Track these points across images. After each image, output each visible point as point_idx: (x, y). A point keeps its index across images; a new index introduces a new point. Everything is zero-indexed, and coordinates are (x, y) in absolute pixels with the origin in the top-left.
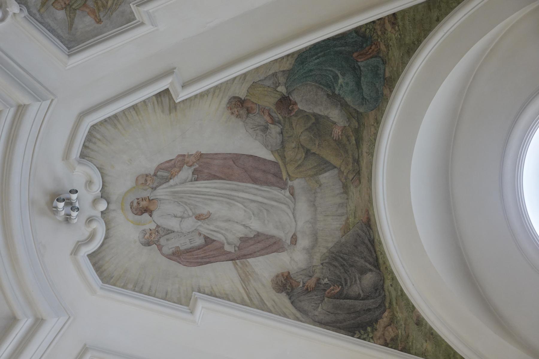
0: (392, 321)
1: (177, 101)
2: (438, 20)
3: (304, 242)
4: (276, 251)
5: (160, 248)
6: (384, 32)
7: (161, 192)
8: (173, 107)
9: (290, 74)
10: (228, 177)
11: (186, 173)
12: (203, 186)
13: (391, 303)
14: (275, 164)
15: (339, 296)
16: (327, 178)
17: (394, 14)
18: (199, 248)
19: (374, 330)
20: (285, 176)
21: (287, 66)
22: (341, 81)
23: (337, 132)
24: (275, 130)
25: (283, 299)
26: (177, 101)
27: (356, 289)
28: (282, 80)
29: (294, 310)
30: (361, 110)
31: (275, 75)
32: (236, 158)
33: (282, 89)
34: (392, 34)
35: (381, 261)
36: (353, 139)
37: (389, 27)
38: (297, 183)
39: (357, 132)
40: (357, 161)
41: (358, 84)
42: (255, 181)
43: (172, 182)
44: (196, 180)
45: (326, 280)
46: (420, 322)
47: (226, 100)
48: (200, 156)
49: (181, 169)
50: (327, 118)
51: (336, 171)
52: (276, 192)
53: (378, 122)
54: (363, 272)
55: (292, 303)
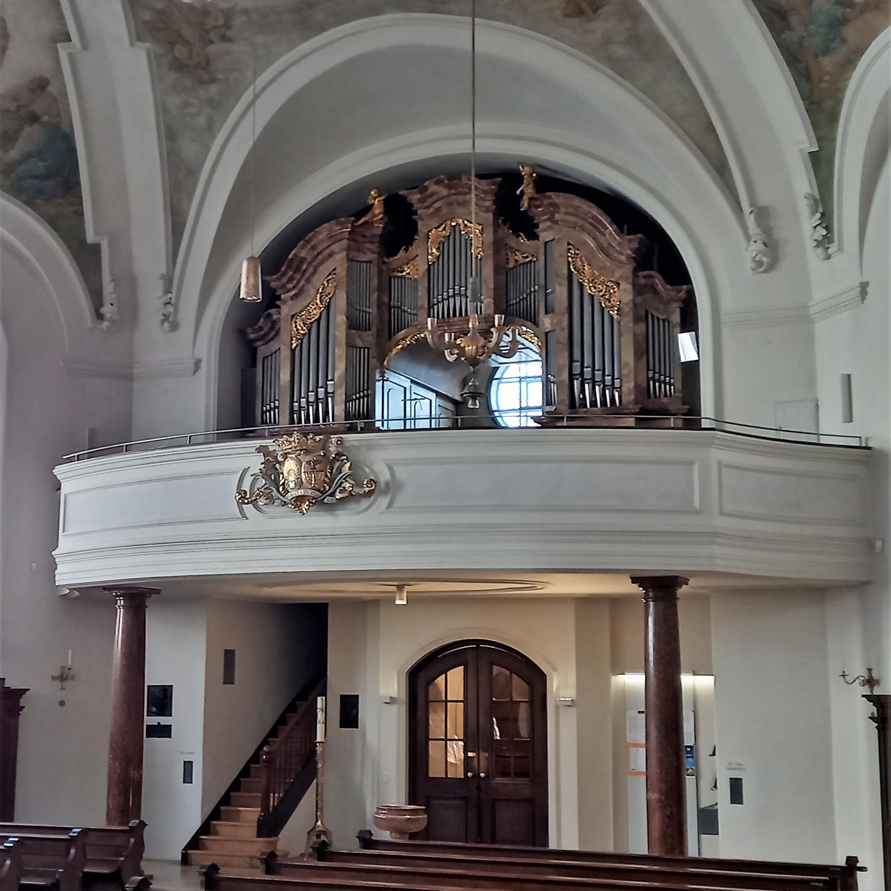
2: (69, 247)
9: (57, 127)
17: (83, 214)
21: (65, 127)
22: (40, 164)
24: (13, 106)
30: (13, 175)
31: (59, 115)
33: (46, 118)
37: (75, 208)
41: (36, 177)
47: (48, 76)
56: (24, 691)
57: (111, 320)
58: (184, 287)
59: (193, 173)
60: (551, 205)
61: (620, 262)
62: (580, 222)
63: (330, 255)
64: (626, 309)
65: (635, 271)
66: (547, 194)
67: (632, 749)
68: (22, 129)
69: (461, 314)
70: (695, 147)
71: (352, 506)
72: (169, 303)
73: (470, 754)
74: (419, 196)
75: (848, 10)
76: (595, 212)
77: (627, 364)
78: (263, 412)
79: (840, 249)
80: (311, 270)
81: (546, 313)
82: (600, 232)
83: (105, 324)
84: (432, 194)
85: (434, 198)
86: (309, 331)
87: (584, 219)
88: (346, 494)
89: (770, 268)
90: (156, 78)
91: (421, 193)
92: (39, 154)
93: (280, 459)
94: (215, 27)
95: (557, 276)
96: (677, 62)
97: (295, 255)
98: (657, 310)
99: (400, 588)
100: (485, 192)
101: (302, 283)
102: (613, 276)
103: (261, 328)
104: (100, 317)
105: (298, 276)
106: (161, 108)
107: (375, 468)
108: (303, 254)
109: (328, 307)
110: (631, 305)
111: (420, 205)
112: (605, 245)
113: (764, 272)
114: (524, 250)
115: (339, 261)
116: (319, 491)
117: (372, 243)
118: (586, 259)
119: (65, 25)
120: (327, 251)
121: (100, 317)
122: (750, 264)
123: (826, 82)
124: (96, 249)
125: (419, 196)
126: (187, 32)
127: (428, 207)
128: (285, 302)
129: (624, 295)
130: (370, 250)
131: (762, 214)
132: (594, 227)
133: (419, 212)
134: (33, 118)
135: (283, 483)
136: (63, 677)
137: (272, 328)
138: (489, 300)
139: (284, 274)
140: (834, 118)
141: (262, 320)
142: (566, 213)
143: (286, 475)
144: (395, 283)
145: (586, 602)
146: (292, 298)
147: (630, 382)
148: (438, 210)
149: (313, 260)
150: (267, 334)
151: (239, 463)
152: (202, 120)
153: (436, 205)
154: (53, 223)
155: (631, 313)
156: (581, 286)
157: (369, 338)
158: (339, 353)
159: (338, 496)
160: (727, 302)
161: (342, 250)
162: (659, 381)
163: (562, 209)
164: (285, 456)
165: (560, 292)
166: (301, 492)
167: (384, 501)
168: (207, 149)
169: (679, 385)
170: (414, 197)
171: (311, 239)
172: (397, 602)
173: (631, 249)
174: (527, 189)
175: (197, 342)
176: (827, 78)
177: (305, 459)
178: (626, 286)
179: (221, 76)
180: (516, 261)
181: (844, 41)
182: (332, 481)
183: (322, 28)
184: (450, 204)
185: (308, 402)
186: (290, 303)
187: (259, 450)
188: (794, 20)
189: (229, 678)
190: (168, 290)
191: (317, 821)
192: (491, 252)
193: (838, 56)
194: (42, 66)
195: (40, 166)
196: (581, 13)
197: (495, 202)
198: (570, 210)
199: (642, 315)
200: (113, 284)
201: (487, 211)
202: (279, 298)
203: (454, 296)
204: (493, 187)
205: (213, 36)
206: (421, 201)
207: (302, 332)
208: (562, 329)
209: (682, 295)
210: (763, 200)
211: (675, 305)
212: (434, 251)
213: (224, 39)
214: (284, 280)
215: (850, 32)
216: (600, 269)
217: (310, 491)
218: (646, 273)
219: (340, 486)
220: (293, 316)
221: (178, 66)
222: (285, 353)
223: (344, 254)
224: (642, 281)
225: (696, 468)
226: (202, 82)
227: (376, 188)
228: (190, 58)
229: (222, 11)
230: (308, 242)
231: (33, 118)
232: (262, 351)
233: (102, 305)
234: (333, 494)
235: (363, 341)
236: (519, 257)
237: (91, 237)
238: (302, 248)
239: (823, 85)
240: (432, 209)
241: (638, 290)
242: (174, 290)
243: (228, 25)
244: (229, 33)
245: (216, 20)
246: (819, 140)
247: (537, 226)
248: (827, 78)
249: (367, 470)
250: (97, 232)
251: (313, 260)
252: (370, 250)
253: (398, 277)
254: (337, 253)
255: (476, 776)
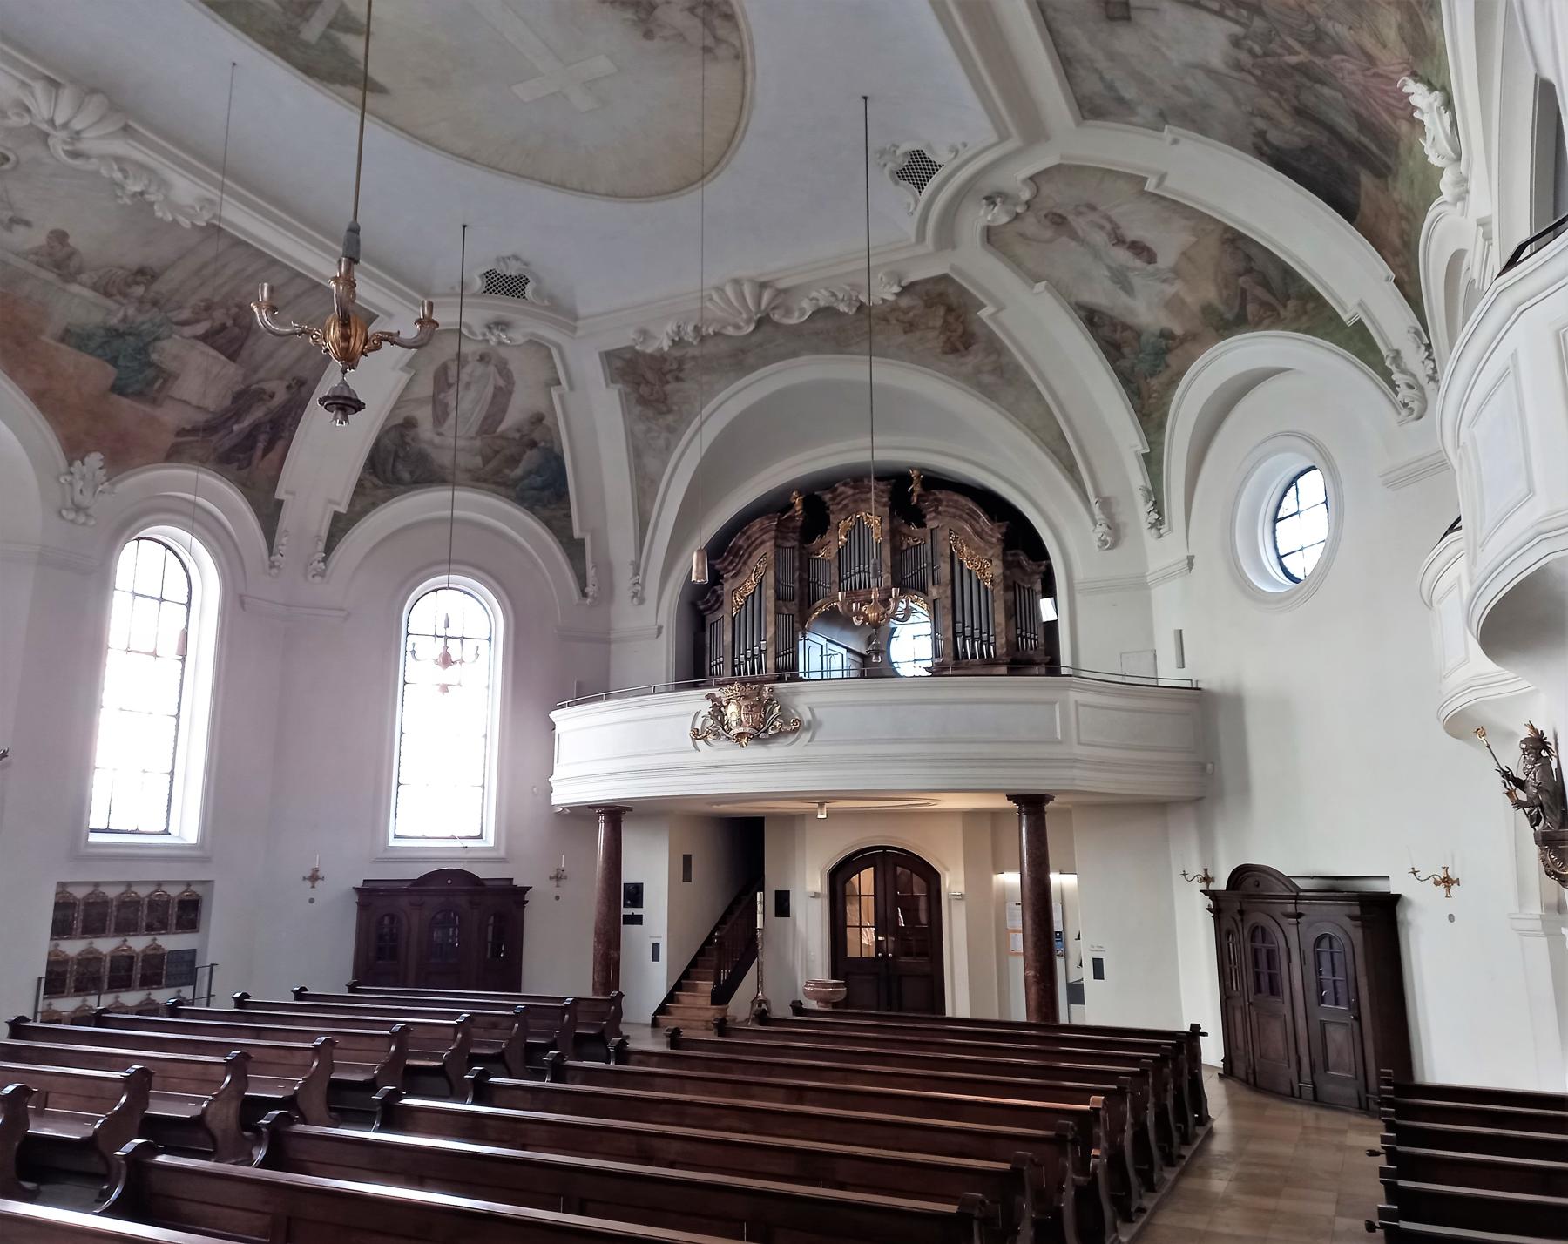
0: (376, 487)
1: (552, 389)
2: (561, 542)
3: (437, 440)
4: (434, 422)
5: (453, 360)
6: (562, 509)
7: (492, 368)
8: (548, 385)
9: (551, 450)
10: (492, 403)
11: (501, 383)
12: (490, 391)
13: (388, 487)
14: (494, 432)
15: (396, 456)
16: (478, 461)
17: (571, 516)
18: (446, 379)
19: (370, 474)
20: (485, 436)
21: (556, 450)
23: (507, 471)
24: (517, 436)
25: (399, 420)
26: (552, 389)
27: (400, 466)
28: (548, 445)
29: (390, 426)
30: (518, 488)
31: (552, 441)
32: (504, 411)
33: (542, 444)
34: (559, 513)
35: (418, 485)
36: (500, 480)
38: (478, 443)
39: (504, 484)
40: (485, 481)
41: (535, 489)
42: (485, 419)
43: (498, 376)
44: (495, 388)
45: (408, 449)
46: (374, 505)
48: (510, 393)
49: (505, 380)
50: (517, 467)
51: (481, 466)
52: (475, 429)
53: (508, 497)
54: (412, 473)
55: (395, 426)
56: (528, 888)
57: (593, 597)
58: (649, 569)
59: (655, 483)
60: (936, 500)
61: (992, 544)
62: (959, 513)
63: (762, 543)
64: (998, 580)
65: (1004, 551)
66: (933, 491)
67: (1012, 935)
68: (525, 452)
69: (865, 587)
70: (1050, 453)
71: (782, 740)
72: (638, 583)
73: (880, 938)
74: (830, 495)
75: (1171, 342)
76: (971, 504)
77: (1000, 624)
78: (711, 667)
79: (1170, 529)
80: (746, 555)
81: (933, 585)
82: (974, 519)
83: (588, 601)
84: (841, 494)
85: (843, 496)
86: (746, 602)
87: (962, 510)
88: (777, 731)
89: (1114, 546)
90: (626, 411)
91: (832, 492)
92: (538, 472)
93: (724, 704)
94: (670, 371)
95: (942, 555)
96: (1033, 385)
97: (734, 543)
98: (1023, 580)
99: (821, 805)
100: (883, 491)
101: (740, 565)
102: (986, 555)
103: (708, 601)
104: (584, 595)
105: (737, 560)
106: (630, 434)
107: (799, 710)
108: (741, 542)
109: (760, 584)
110: (1001, 577)
111: (831, 503)
112: (980, 530)
113: (1108, 549)
114: (916, 535)
115: (768, 548)
116: (755, 728)
117: (795, 533)
118: (965, 542)
119: (556, 373)
120: (758, 542)
121: (584, 595)
122: (1097, 543)
123: (1155, 398)
124: (581, 543)
125: (830, 495)
126: (650, 376)
127: (838, 504)
128: (727, 580)
129: (995, 569)
130: (793, 539)
131: (1105, 503)
132: (971, 516)
133: (831, 507)
134: (533, 444)
135: (727, 723)
136: (558, 877)
137: (716, 601)
138: (887, 575)
139: (726, 558)
140: (1161, 426)
141: (709, 595)
142: (947, 506)
143: (729, 716)
144: (812, 564)
145: (971, 815)
146: (732, 577)
147: (1002, 638)
148: (846, 505)
149: (748, 547)
150: (713, 605)
151: (694, 707)
152: (661, 442)
153: (844, 502)
154: (548, 523)
155: (1002, 584)
156: (961, 563)
157: (793, 606)
158: (770, 619)
159: (771, 732)
160: (1079, 574)
161: (771, 539)
162: (1026, 637)
163: (945, 503)
164: (728, 701)
165: (944, 569)
166: (741, 730)
167: (806, 736)
168: (665, 465)
169: (1042, 641)
170: (827, 497)
171: (747, 531)
172: (819, 816)
173: (1001, 534)
174: (916, 488)
175: (660, 611)
176: (1154, 395)
177: (744, 703)
178: (997, 562)
179: (675, 408)
180: (909, 544)
181: (1167, 366)
182: (765, 720)
183: (753, 369)
184: (855, 501)
185: (746, 658)
186: (731, 581)
187: (708, 697)
188: (1126, 350)
189: (687, 877)
190: (636, 574)
191: (758, 992)
192: (888, 538)
193: (1164, 378)
194: (540, 405)
195: (538, 481)
196: (954, 350)
197: (890, 499)
198: (951, 503)
199: (1010, 586)
200: (594, 569)
201: (885, 505)
202: (722, 577)
203: (859, 572)
204: (889, 487)
205: (669, 377)
206: (833, 499)
207: (740, 603)
208: (947, 597)
209: (1043, 568)
210: (1106, 492)
211: (1037, 576)
212: (843, 537)
213: (678, 379)
214: (726, 563)
215: (1171, 359)
216: (975, 549)
217: (748, 729)
218: (1013, 552)
219: (772, 724)
220: (733, 591)
221: (643, 401)
222: (728, 620)
223: (773, 542)
224: (1010, 558)
225: (1057, 706)
226: (661, 413)
227: (797, 490)
228: (652, 395)
229: (675, 358)
230: (744, 533)
231: (533, 444)
232: (710, 618)
233: (586, 586)
234: (766, 731)
235: (788, 609)
236: (911, 541)
237: (577, 534)
238: (740, 538)
239: (1151, 401)
240: (840, 506)
241: (1007, 565)
242: (641, 573)
243: (680, 369)
244: (681, 375)
245: (671, 365)
246: (1150, 443)
247: (925, 516)
248: (1154, 395)
249: (793, 711)
250: (582, 529)
251: (748, 547)
252: (793, 539)
253: (815, 559)
254: (768, 541)
255: (885, 955)
